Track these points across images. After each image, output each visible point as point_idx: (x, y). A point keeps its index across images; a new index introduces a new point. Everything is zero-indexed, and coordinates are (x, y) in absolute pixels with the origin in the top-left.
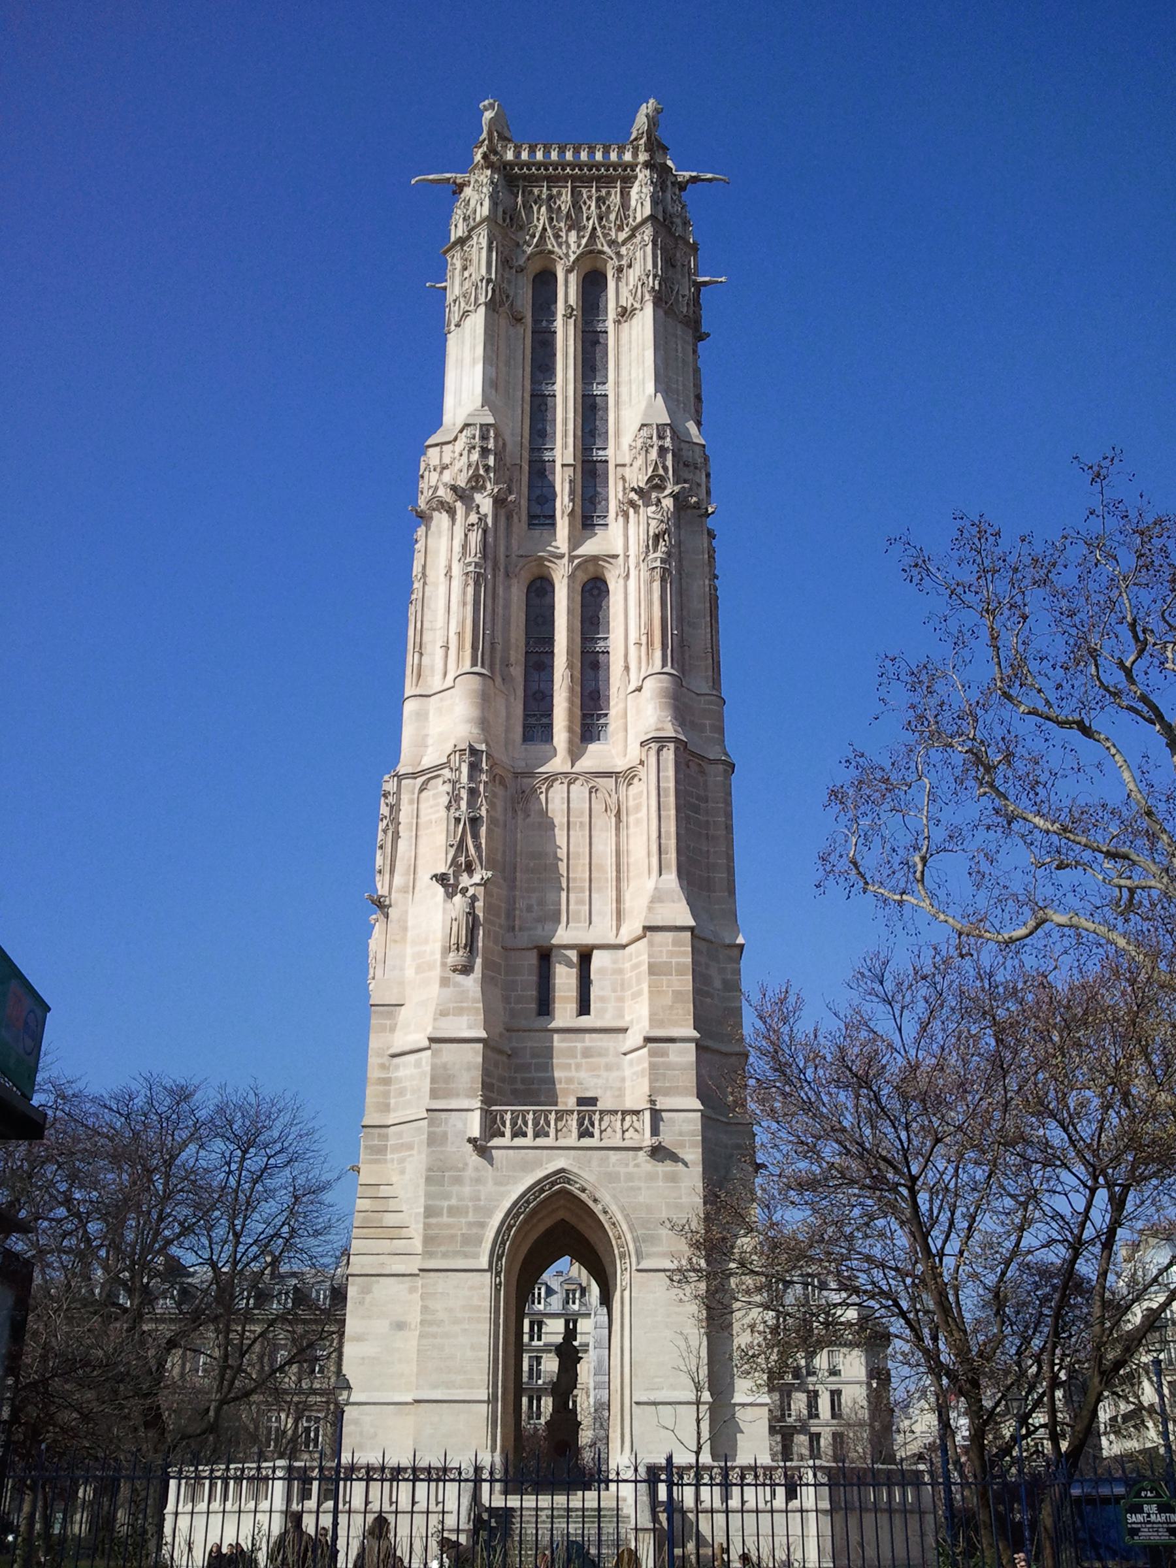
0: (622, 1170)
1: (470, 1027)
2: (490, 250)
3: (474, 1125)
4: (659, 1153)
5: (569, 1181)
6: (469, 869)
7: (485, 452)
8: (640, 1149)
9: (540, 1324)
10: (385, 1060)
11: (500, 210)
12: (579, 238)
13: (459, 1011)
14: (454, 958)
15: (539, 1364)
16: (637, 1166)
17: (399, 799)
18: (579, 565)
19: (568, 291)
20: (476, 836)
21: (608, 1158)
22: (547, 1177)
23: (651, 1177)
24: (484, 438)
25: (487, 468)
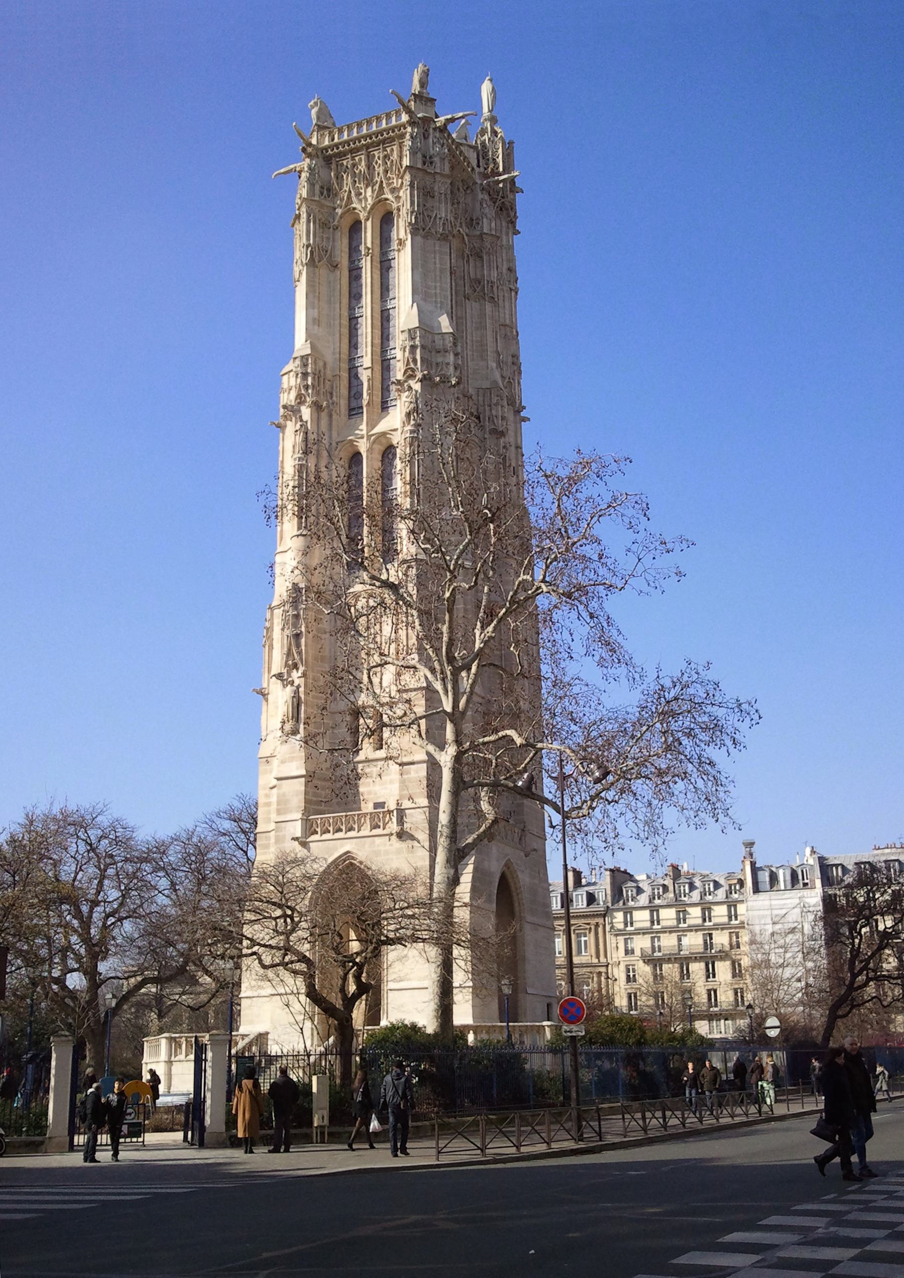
0: (382, 848)
1: (297, 769)
2: (308, 221)
3: (297, 829)
4: (402, 835)
5: (353, 858)
6: (295, 666)
7: (305, 375)
8: (392, 834)
9: (710, 909)
10: (267, 791)
11: (317, 187)
12: (373, 191)
13: (292, 759)
14: (288, 727)
15: (711, 939)
16: (391, 845)
17: (272, 624)
18: (374, 442)
19: (368, 236)
20: (298, 645)
21: (374, 842)
22: (340, 857)
23: (399, 852)
24: (305, 365)
25: (307, 387)
